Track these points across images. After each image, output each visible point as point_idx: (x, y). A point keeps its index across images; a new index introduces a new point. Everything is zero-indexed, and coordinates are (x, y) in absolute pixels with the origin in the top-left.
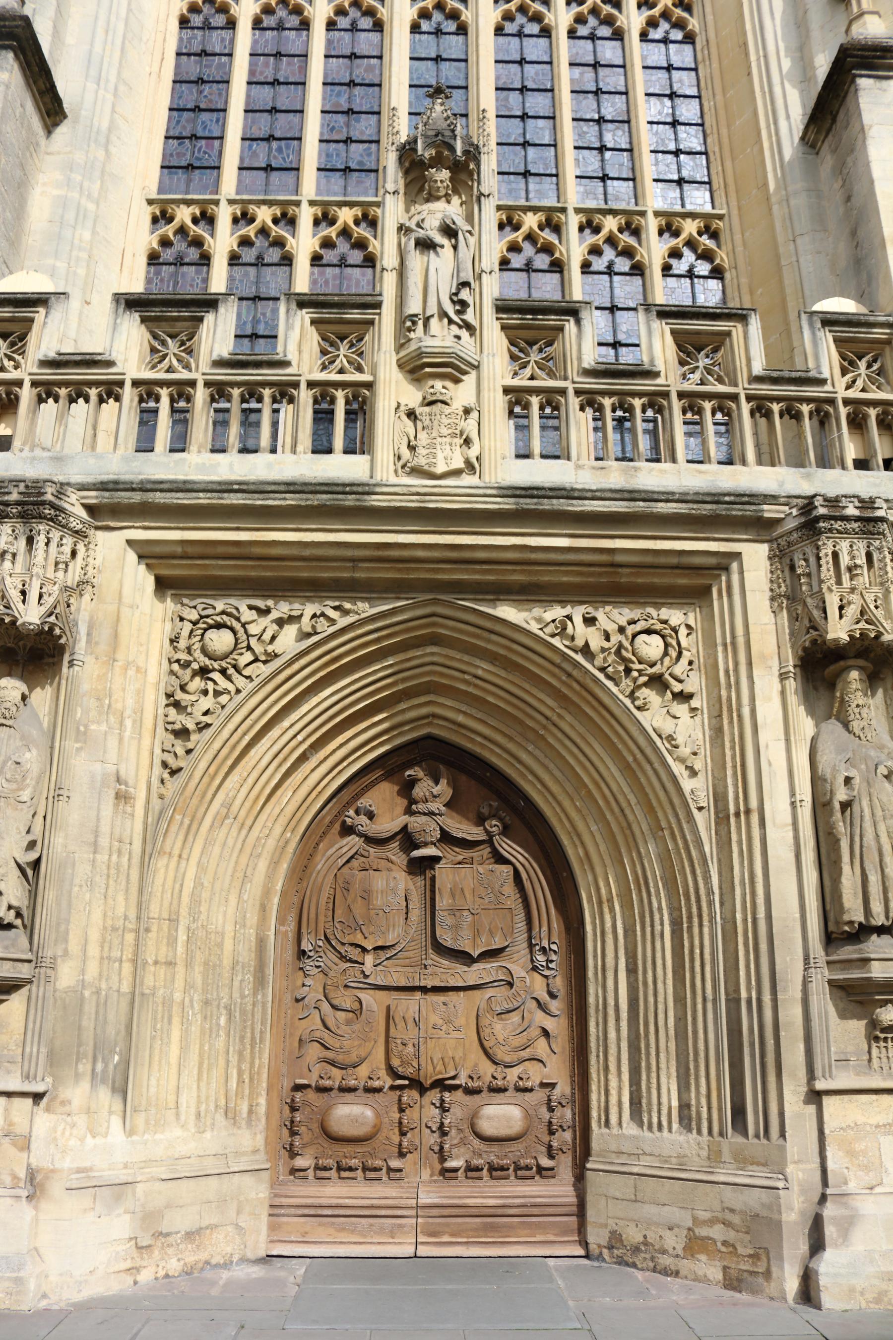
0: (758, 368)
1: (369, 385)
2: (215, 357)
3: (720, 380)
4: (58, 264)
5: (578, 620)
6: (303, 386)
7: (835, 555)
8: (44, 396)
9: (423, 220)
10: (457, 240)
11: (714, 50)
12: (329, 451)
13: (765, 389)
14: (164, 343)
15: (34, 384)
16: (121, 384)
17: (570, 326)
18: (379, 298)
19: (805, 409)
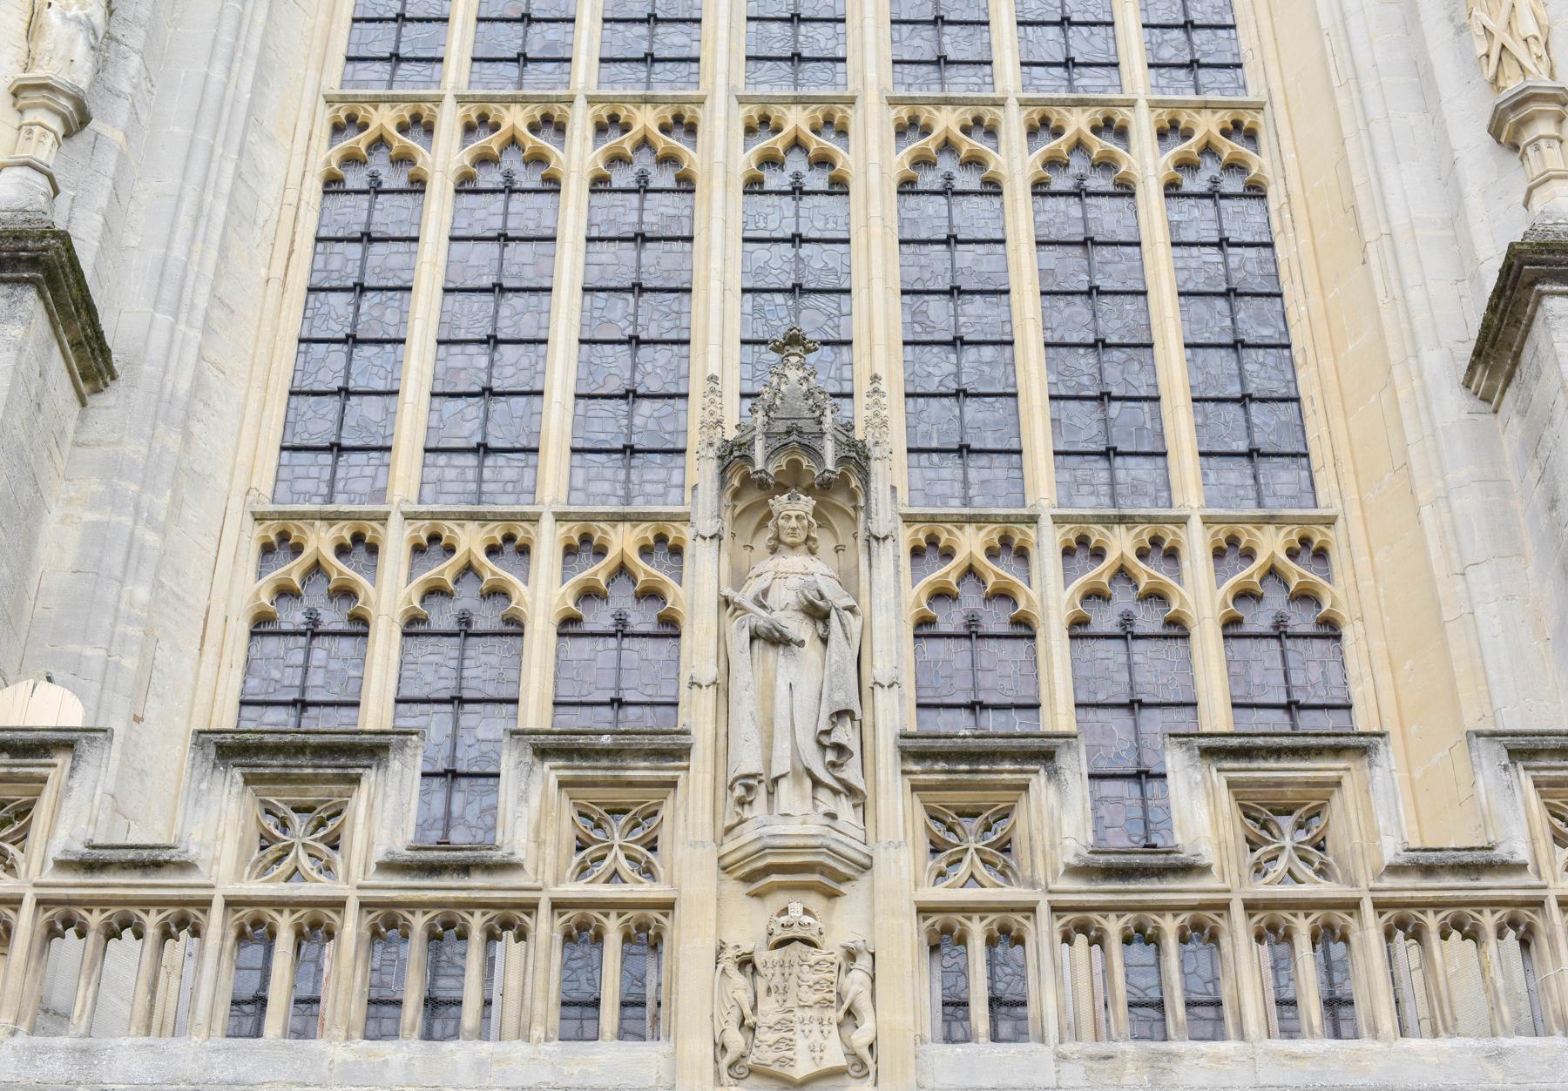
0: (1390, 852)
1: (668, 906)
2: (379, 854)
3: (1322, 872)
4: (88, 651)
6: (544, 908)
8: (60, 927)
9: (765, 593)
10: (826, 626)
11: (1300, 213)
13: (1410, 887)
14: (284, 825)
15: (41, 903)
16: (205, 905)
17: (1039, 782)
18: (683, 739)
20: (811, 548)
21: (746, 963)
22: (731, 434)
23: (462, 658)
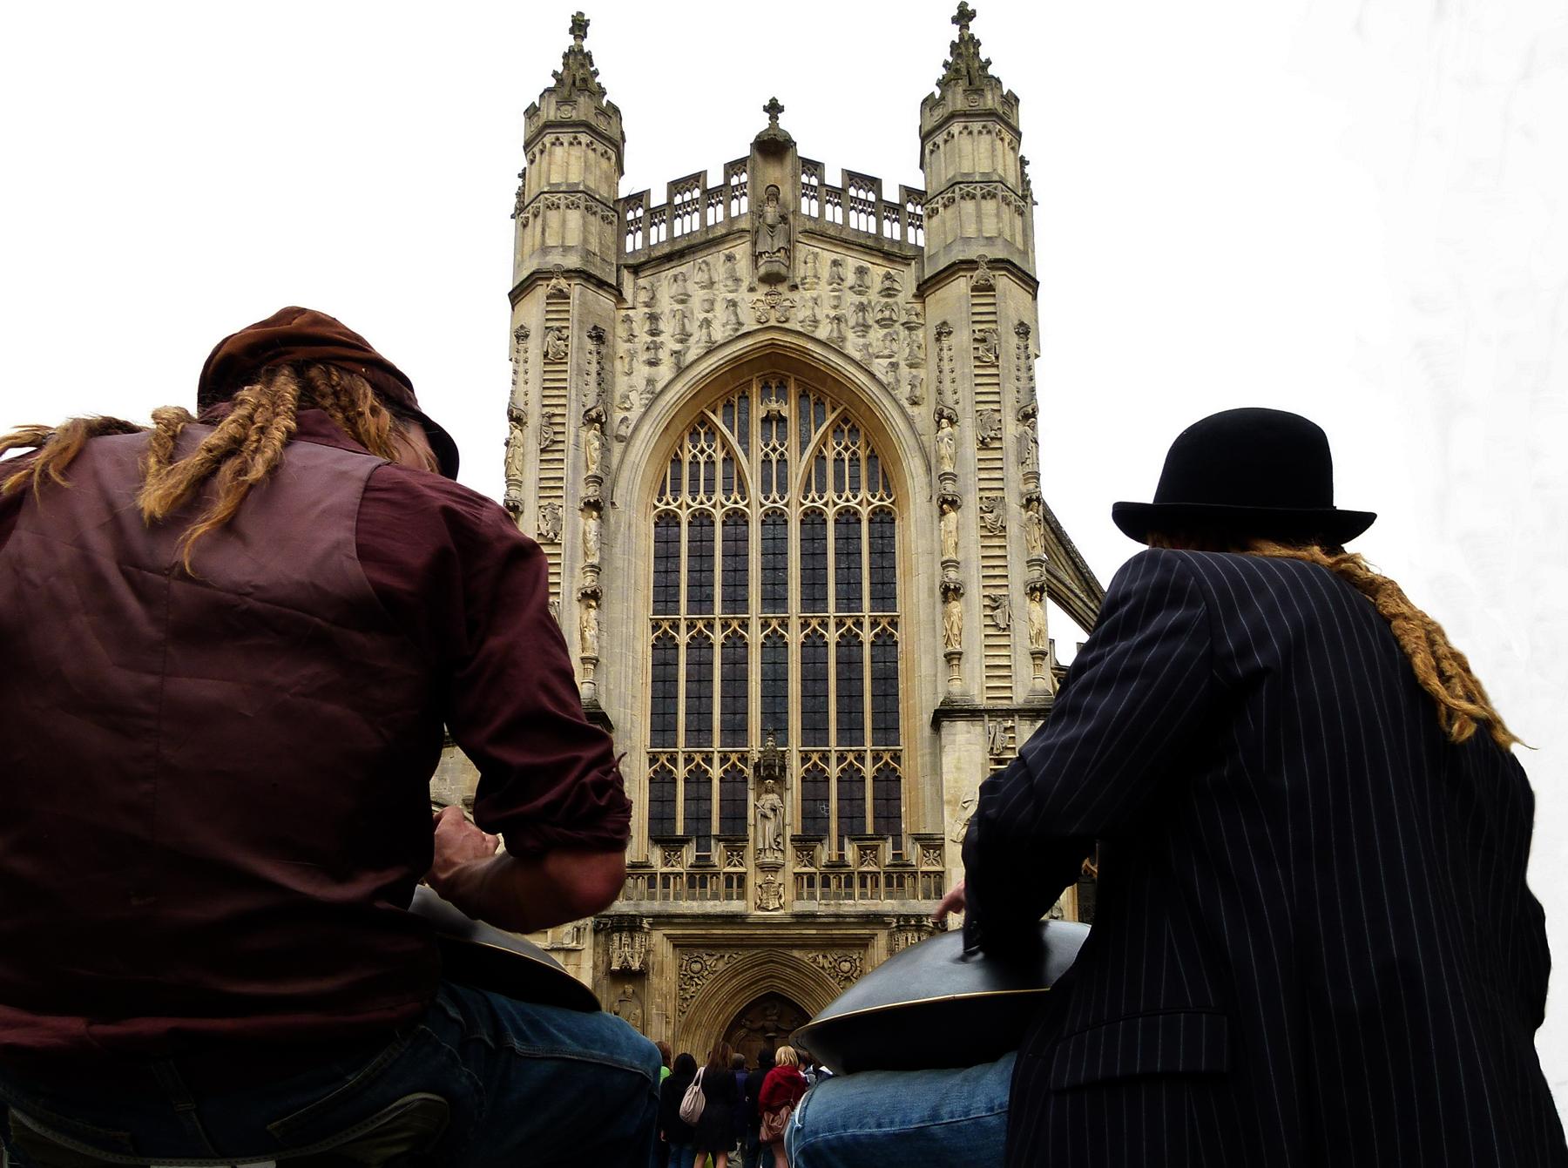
1: (745, 873)
2: (689, 863)
3: (876, 864)
5: (821, 957)
7: (907, 938)
12: (732, 899)
13: (890, 869)
17: (819, 846)
19: (906, 876)
20: (773, 792)
21: (760, 886)
22: (757, 760)
23: (698, 788)
